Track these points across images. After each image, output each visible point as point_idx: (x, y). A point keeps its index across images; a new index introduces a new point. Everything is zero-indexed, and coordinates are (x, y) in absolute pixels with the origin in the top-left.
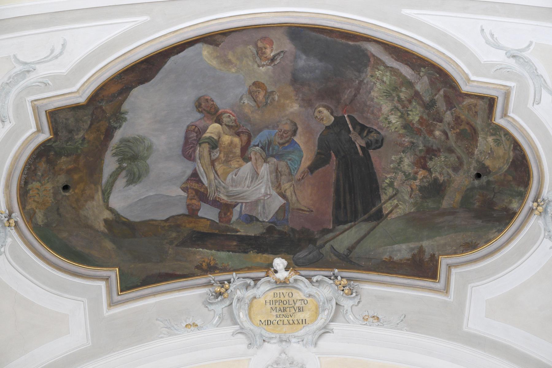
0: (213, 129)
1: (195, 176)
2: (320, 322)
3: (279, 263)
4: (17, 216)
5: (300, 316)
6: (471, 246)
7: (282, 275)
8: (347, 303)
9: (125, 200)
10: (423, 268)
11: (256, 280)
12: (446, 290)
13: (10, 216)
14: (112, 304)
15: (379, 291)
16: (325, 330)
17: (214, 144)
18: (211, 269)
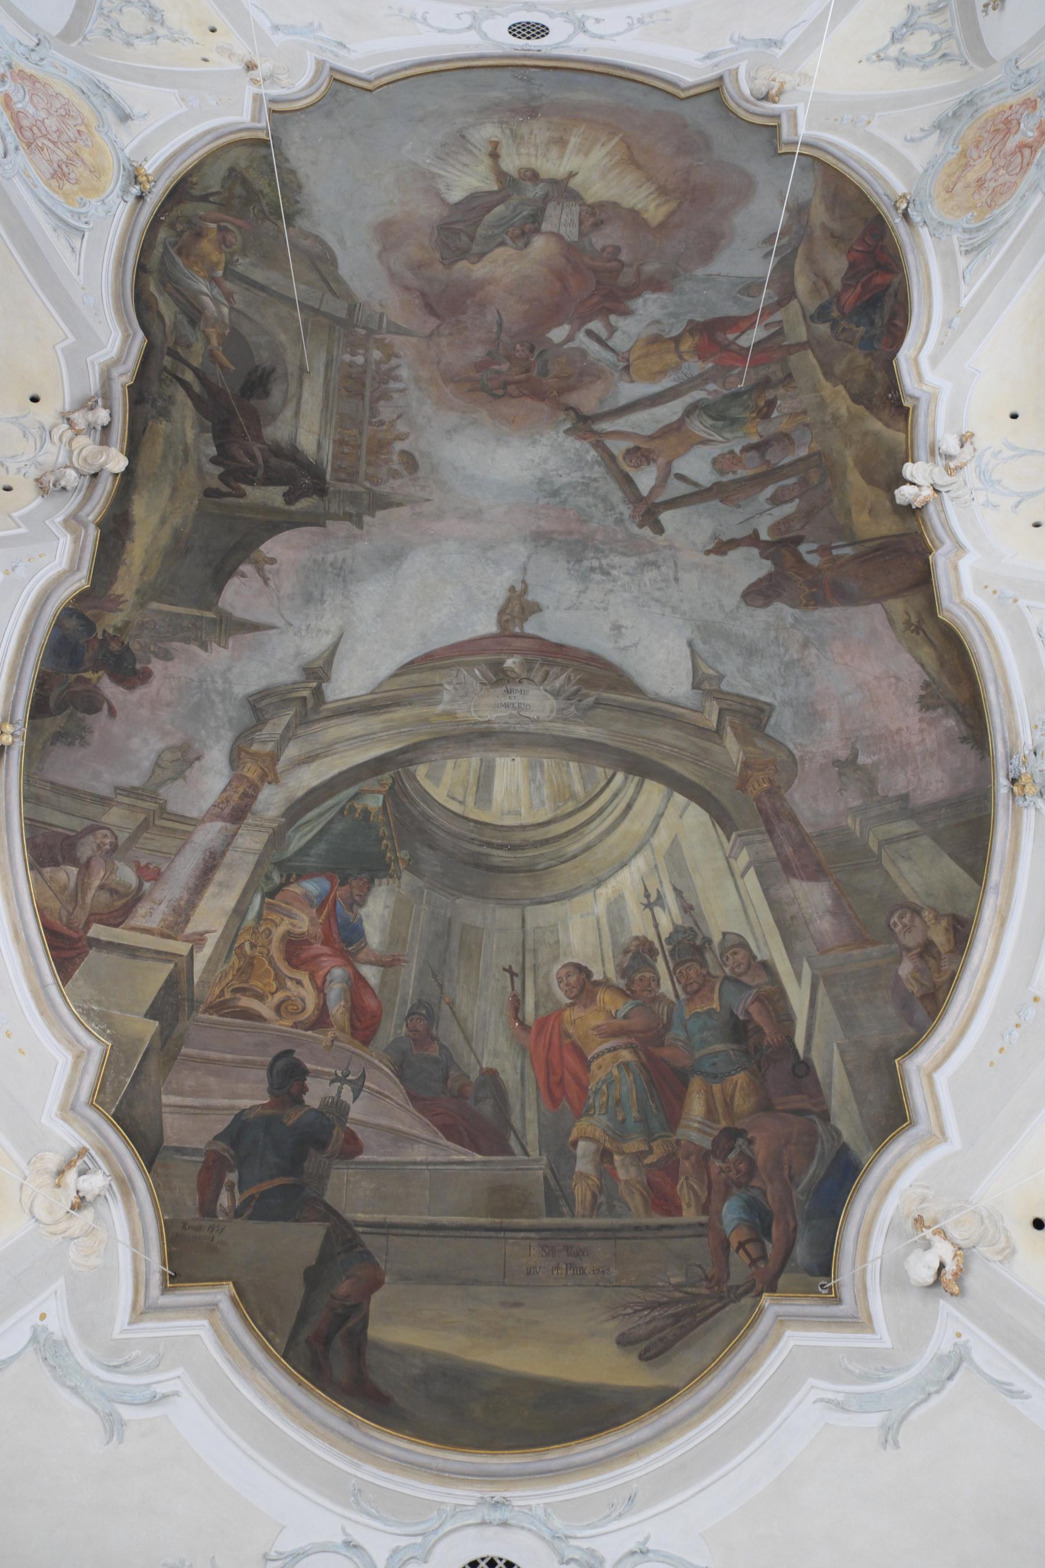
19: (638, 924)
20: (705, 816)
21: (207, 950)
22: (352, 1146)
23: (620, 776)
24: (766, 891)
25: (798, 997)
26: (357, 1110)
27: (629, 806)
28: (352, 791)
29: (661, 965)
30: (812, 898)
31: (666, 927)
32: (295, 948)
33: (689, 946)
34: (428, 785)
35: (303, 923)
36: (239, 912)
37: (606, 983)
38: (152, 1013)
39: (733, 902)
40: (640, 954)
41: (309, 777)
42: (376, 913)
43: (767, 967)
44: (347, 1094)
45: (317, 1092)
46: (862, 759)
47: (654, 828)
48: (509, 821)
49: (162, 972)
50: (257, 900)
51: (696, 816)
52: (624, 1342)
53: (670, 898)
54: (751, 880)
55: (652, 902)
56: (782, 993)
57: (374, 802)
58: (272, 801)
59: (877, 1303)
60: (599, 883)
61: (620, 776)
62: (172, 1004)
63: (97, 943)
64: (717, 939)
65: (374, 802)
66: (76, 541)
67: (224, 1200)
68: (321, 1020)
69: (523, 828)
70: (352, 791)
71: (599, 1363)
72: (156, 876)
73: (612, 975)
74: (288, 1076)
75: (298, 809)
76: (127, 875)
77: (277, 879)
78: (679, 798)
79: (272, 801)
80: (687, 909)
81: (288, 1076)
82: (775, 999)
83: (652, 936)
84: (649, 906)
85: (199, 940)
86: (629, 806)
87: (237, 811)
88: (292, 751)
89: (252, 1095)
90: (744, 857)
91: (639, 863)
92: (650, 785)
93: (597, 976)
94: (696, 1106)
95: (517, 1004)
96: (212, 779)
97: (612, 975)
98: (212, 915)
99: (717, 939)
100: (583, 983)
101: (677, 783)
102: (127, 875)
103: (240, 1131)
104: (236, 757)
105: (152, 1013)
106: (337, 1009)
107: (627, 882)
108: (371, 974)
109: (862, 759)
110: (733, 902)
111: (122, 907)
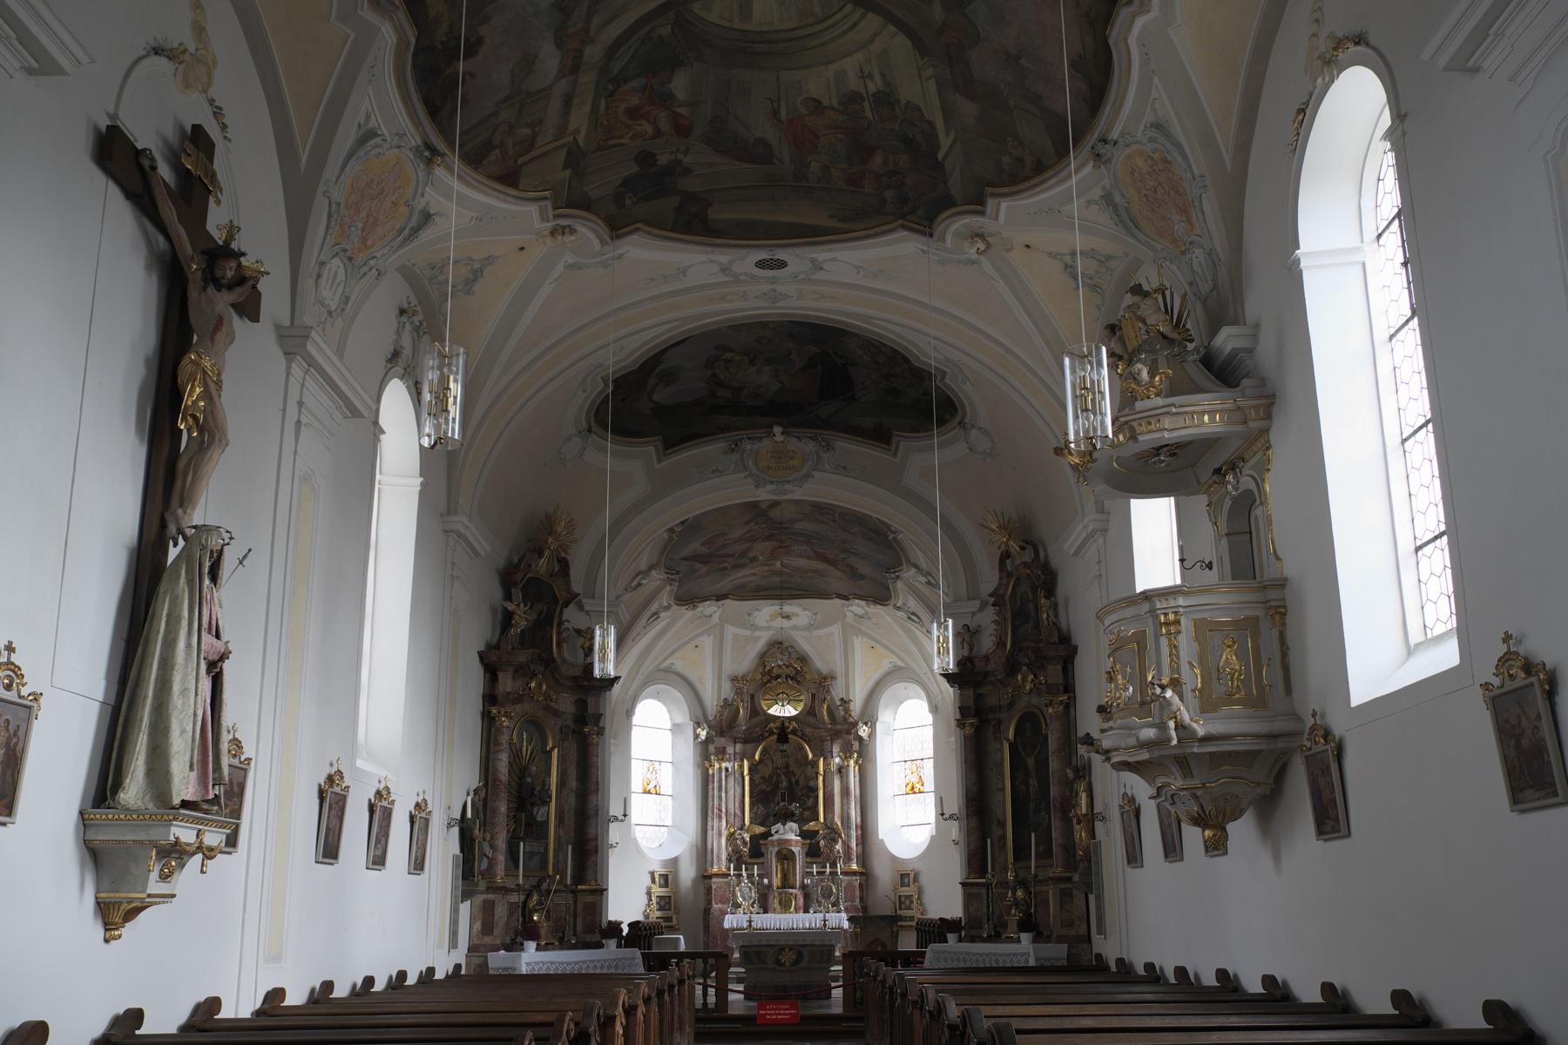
0: (728, 355)
1: (714, 375)
2: (805, 470)
3: (777, 430)
4: (595, 428)
5: (792, 463)
6: (917, 430)
7: (779, 438)
8: (825, 456)
9: (661, 395)
10: (881, 437)
11: (760, 439)
12: (895, 455)
13: (589, 431)
14: (659, 461)
15: (847, 447)
16: (808, 476)
17: (727, 361)
18: (727, 429)
19: (854, 84)
20: (909, 43)
21: (583, 133)
22: (687, 171)
23: (849, 7)
24: (940, 93)
25: (945, 142)
26: (687, 160)
27: (855, 25)
28: (648, 28)
29: (866, 105)
30: (968, 109)
31: (872, 88)
32: (633, 113)
33: (886, 100)
34: (703, 14)
35: (634, 101)
36: (595, 109)
37: (832, 108)
38: (564, 168)
39: (918, 88)
40: (856, 98)
41: (614, 30)
42: (680, 84)
43: (931, 124)
44: (680, 156)
45: (663, 160)
46: (1022, 61)
47: (872, 40)
48: (764, 28)
49: (563, 153)
50: (603, 101)
51: (902, 40)
52: (830, 216)
53: (877, 76)
54: (932, 85)
55: (864, 76)
56: (936, 136)
57: (665, 31)
58: (593, 53)
59: (949, 238)
60: (831, 62)
61: (849, 7)
62: (575, 159)
63: (525, 164)
64: (903, 102)
65: (665, 31)
66: (391, 19)
67: (628, 202)
68: (658, 134)
69: (776, 32)
70: (648, 28)
71: (820, 220)
72: (540, 122)
73: (835, 103)
74: (646, 158)
75: (611, 52)
76: (527, 131)
77: (611, 87)
78: (892, 28)
79: (593, 53)
80: (887, 84)
81: (646, 158)
82: (932, 136)
83: (862, 91)
84: (863, 77)
85: (577, 131)
86: (855, 25)
87: (573, 66)
88: (597, 20)
89: (632, 169)
90: (930, 72)
91: (859, 56)
92: (870, 15)
93: (826, 103)
94: (878, 159)
95: (775, 113)
96: (550, 60)
97: (835, 103)
98: (580, 119)
99: (903, 102)
100: (817, 106)
101: (890, 18)
102: (527, 131)
103: (627, 183)
104: (559, 43)
105: (564, 168)
106: (665, 125)
107: (851, 64)
108: (683, 111)
109: (1022, 61)
110: (918, 88)
111: (531, 143)
